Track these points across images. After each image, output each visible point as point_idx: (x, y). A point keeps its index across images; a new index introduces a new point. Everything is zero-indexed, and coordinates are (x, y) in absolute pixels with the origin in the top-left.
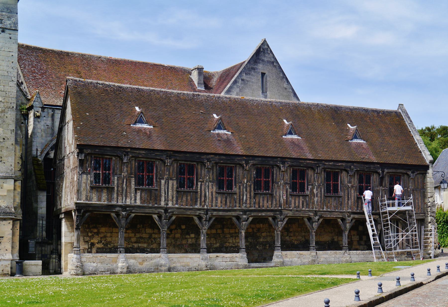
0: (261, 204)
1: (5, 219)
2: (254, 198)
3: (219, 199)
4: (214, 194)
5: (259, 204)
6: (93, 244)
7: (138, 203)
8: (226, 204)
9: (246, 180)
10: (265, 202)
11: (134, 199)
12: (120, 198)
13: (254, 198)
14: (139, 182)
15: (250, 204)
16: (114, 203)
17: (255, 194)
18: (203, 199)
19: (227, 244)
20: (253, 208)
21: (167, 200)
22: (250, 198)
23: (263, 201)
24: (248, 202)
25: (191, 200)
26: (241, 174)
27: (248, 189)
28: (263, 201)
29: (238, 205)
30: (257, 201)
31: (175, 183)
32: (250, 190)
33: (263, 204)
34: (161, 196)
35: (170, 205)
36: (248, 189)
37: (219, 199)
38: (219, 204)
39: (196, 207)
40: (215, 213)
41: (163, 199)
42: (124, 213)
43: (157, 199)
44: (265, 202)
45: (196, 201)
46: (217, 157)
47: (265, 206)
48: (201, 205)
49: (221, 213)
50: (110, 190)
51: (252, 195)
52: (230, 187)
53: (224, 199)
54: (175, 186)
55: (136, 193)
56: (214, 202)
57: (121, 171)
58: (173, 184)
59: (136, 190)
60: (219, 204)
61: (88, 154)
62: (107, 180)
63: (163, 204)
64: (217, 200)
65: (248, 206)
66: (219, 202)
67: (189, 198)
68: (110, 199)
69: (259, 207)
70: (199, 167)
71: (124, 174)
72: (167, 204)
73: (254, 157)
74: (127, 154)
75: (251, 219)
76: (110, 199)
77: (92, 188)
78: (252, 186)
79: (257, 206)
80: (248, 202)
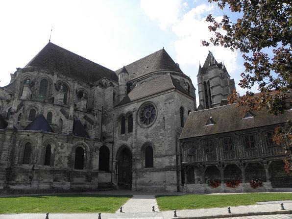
0: (274, 152)
1: (174, 170)
2: (269, 149)
3: (247, 153)
4: (243, 151)
5: (272, 152)
6: (206, 179)
7: (207, 160)
8: (251, 155)
9: (261, 141)
10: (277, 151)
11: (205, 159)
12: (199, 159)
13: (269, 149)
14: (207, 151)
15: (266, 153)
16: (197, 161)
17: (269, 148)
18: (238, 154)
19: (276, 176)
20: (269, 156)
21: (219, 157)
22: (266, 150)
23: (275, 151)
24: (265, 152)
25: (232, 155)
26: (258, 138)
27: (264, 145)
28: (275, 151)
29: (259, 155)
30: (271, 151)
31: (222, 148)
32: (265, 145)
33: (275, 152)
34: (216, 156)
35: (221, 159)
36: (264, 145)
37: (247, 153)
38: (247, 156)
39: (235, 159)
40: (246, 161)
41: (217, 157)
42: (201, 165)
43: (215, 157)
44: (277, 151)
45: (234, 156)
46: (241, 132)
47: (277, 154)
48: (237, 157)
49: (249, 161)
50: (194, 156)
51: (267, 148)
52: (253, 145)
53: (250, 153)
54: (223, 150)
55: (205, 156)
56: (244, 155)
57: (198, 147)
58: (221, 149)
59: (205, 154)
60: (247, 156)
61: (184, 143)
62: (194, 152)
63: (218, 159)
64: (245, 153)
65: (265, 155)
66: (247, 155)
67: (230, 155)
68: (195, 160)
69: (273, 154)
70: (233, 138)
71: (199, 149)
72: (220, 159)
73: (262, 127)
74: (198, 139)
75: (270, 162)
76: (195, 160)
77: (187, 156)
78: (266, 143)
79: (271, 154)
80: (265, 152)
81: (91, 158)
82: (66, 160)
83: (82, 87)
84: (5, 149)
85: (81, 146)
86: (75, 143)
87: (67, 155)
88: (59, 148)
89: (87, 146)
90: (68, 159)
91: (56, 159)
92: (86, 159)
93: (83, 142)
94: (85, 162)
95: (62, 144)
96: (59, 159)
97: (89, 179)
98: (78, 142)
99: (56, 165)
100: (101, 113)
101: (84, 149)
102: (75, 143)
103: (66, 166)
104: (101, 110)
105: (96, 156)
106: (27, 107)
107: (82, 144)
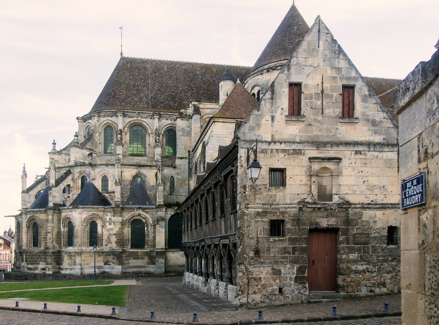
81: (154, 232)
82: (114, 239)
83: (169, 122)
84: (50, 231)
85: (138, 218)
86: (127, 215)
87: (114, 232)
88: (107, 224)
89: (148, 217)
90: (116, 237)
91: (105, 238)
92: (148, 235)
93: (141, 212)
94: (146, 239)
95: (110, 219)
96: (108, 237)
97: (152, 261)
98: (133, 212)
99: (106, 245)
100: (187, 160)
101: (144, 221)
102: (127, 215)
103: (114, 246)
104: (187, 156)
105: (160, 229)
106: (76, 175)
107: (139, 215)
